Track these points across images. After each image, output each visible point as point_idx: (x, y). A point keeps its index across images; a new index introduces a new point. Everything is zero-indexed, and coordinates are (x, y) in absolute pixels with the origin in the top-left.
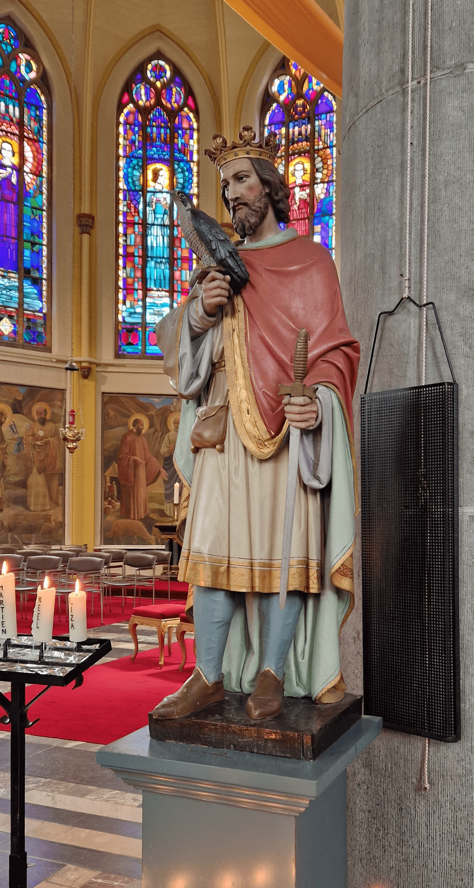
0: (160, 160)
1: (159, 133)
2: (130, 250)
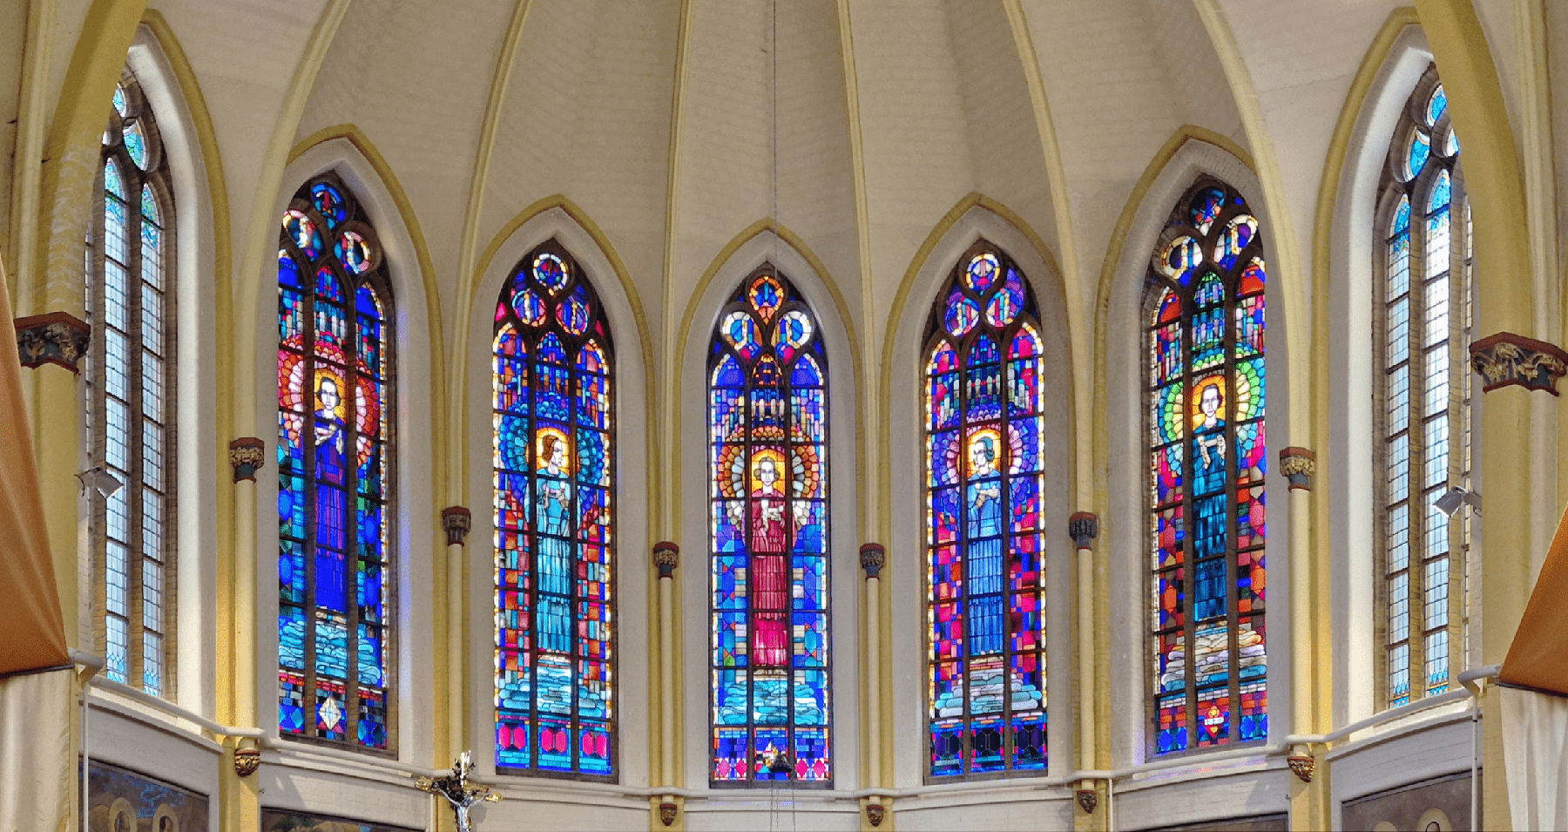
0: (553, 423)
1: (553, 377)
2: (512, 578)
